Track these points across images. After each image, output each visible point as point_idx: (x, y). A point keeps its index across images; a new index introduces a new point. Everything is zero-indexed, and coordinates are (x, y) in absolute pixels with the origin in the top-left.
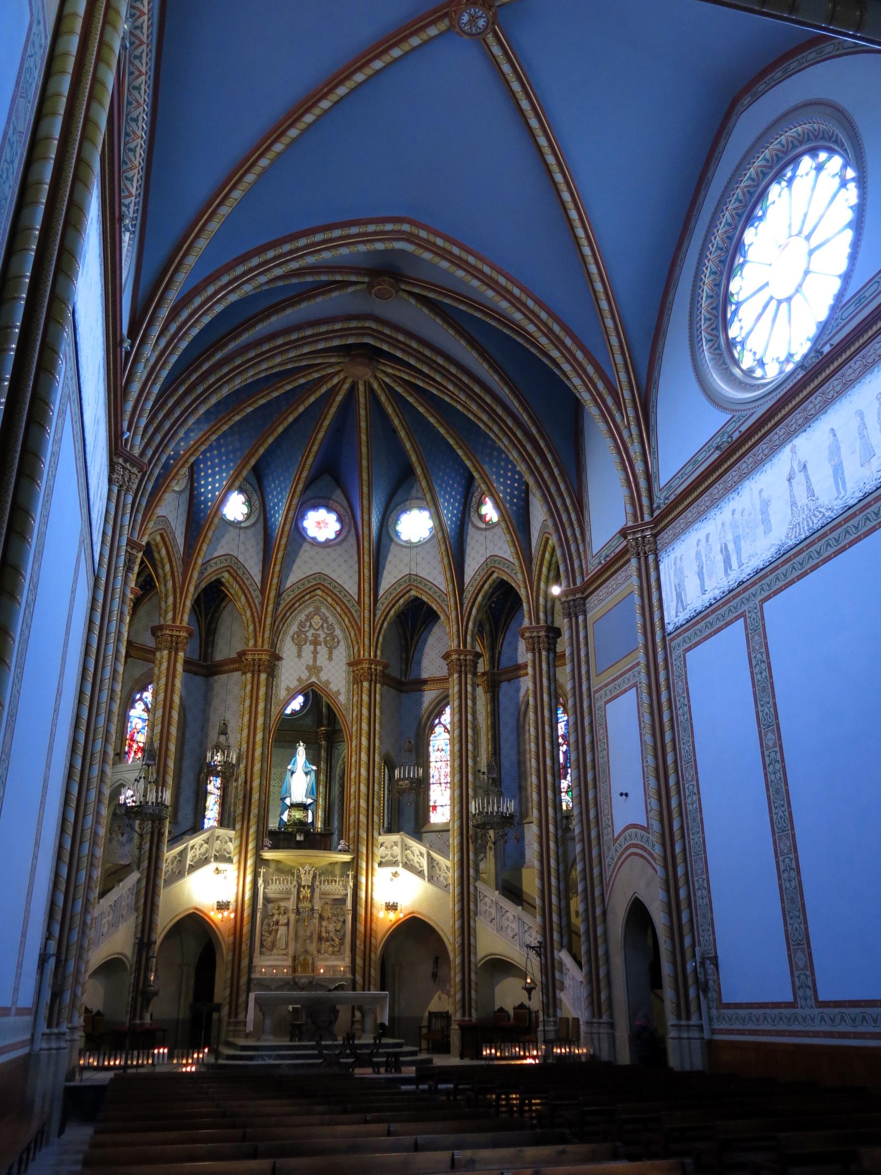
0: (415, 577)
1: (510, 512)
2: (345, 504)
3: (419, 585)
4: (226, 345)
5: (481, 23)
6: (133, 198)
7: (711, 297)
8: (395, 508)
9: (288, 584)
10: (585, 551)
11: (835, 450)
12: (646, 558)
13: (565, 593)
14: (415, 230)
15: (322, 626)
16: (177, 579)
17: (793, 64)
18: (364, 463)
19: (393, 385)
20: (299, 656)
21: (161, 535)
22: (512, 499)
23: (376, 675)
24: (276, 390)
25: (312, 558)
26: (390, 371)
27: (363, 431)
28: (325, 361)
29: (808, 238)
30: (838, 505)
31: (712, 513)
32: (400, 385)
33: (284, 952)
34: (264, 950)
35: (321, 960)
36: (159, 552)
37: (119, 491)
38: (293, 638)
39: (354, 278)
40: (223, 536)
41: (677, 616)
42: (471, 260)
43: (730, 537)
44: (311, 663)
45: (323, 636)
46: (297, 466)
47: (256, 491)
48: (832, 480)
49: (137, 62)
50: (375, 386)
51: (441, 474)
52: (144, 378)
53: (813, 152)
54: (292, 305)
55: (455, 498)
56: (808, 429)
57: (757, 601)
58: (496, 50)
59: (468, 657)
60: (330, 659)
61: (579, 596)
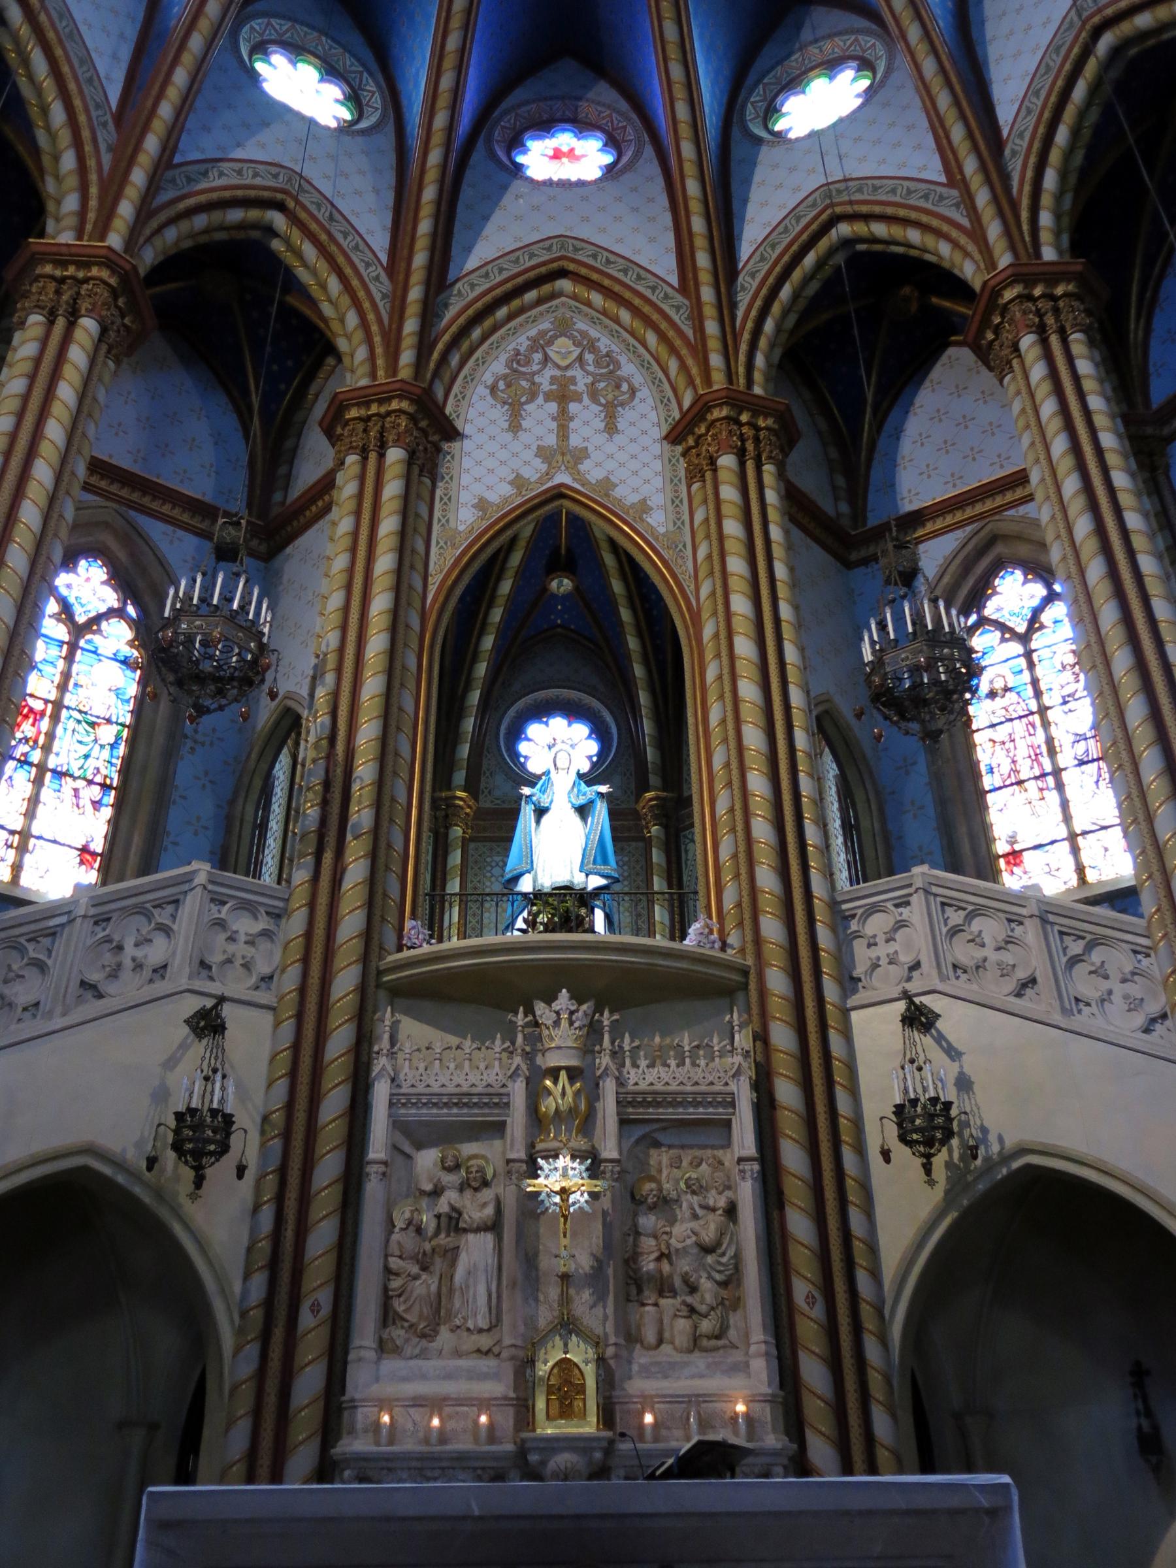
0: (842, 186)
2: (624, 105)
8: (758, 82)
9: (472, 263)
15: (580, 358)
20: (515, 426)
23: (757, 440)
25: (536, 208)
33: (485, 1341)
34: (397, 1333)
35: (646, 1372)
38: (493, 389)
44: (551, 440)
45: (582, 382)
47: (371, 74)
59: (1059, 291)
60: (611, 428)
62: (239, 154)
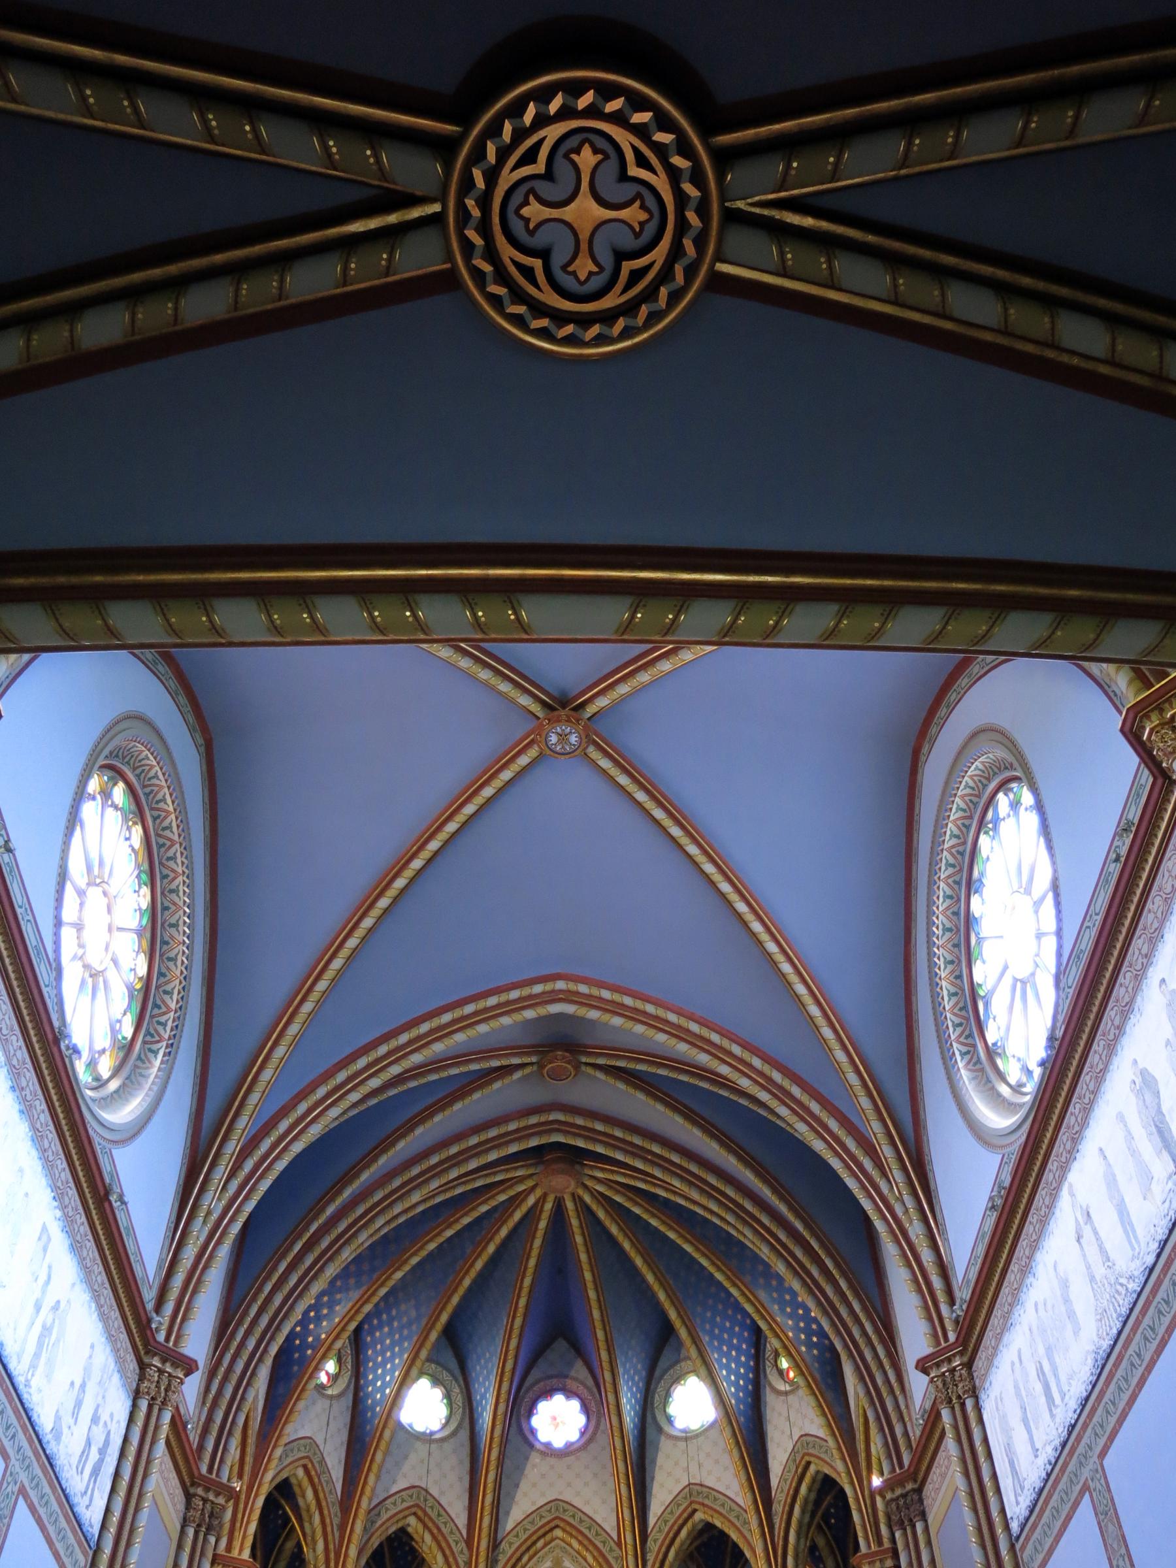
0: (698, 1488)
1: (808, 1358)
2: (590, 1382)
3: (706, 1502)
4: (357, 1175)
5: (573, 739)
6: (172, 1014)
7: (955, 994)
9: (510, 1525)
10: (907, 1407)
11: (1111, 1181)
12: (963, 1405)
13: (889, 1485)
14: (572, 986)
16: (330, 1537)
17: (952, 696)
18: (596, 1314)
19: (608, 1193)
21: (305, 1467)
22: (809, 1337)
24: (449, 1226)
25: (543, 1476)
26: (600, 1175)
27: (586, 1266)
28: (509, 1176)
29: (1028, 891)
30: (1137, 1268)
31: (1016, 1314)
32: (618, 1192)
36: (304, 1496)
37: (150, 1407)
39: (516, 1061)
40: (406, 1457)
41: (1018, 1503)
42: (650, 1008)
43: (1041, 1350)
46: (502, 1332)
47: (456, 1380)
48: (1120, 1230)
49: (171, 864)
50: (587, 1198)
51: (709, 1314)
52: (202, 1239)
53: (1003, 786)
54: (442, 1109)
55: (738, 1349)
56: (1078, 1155)
57: (1095, 1458)
58: (605, 763)
61: (910, 1486)
62: (394, 1489)
